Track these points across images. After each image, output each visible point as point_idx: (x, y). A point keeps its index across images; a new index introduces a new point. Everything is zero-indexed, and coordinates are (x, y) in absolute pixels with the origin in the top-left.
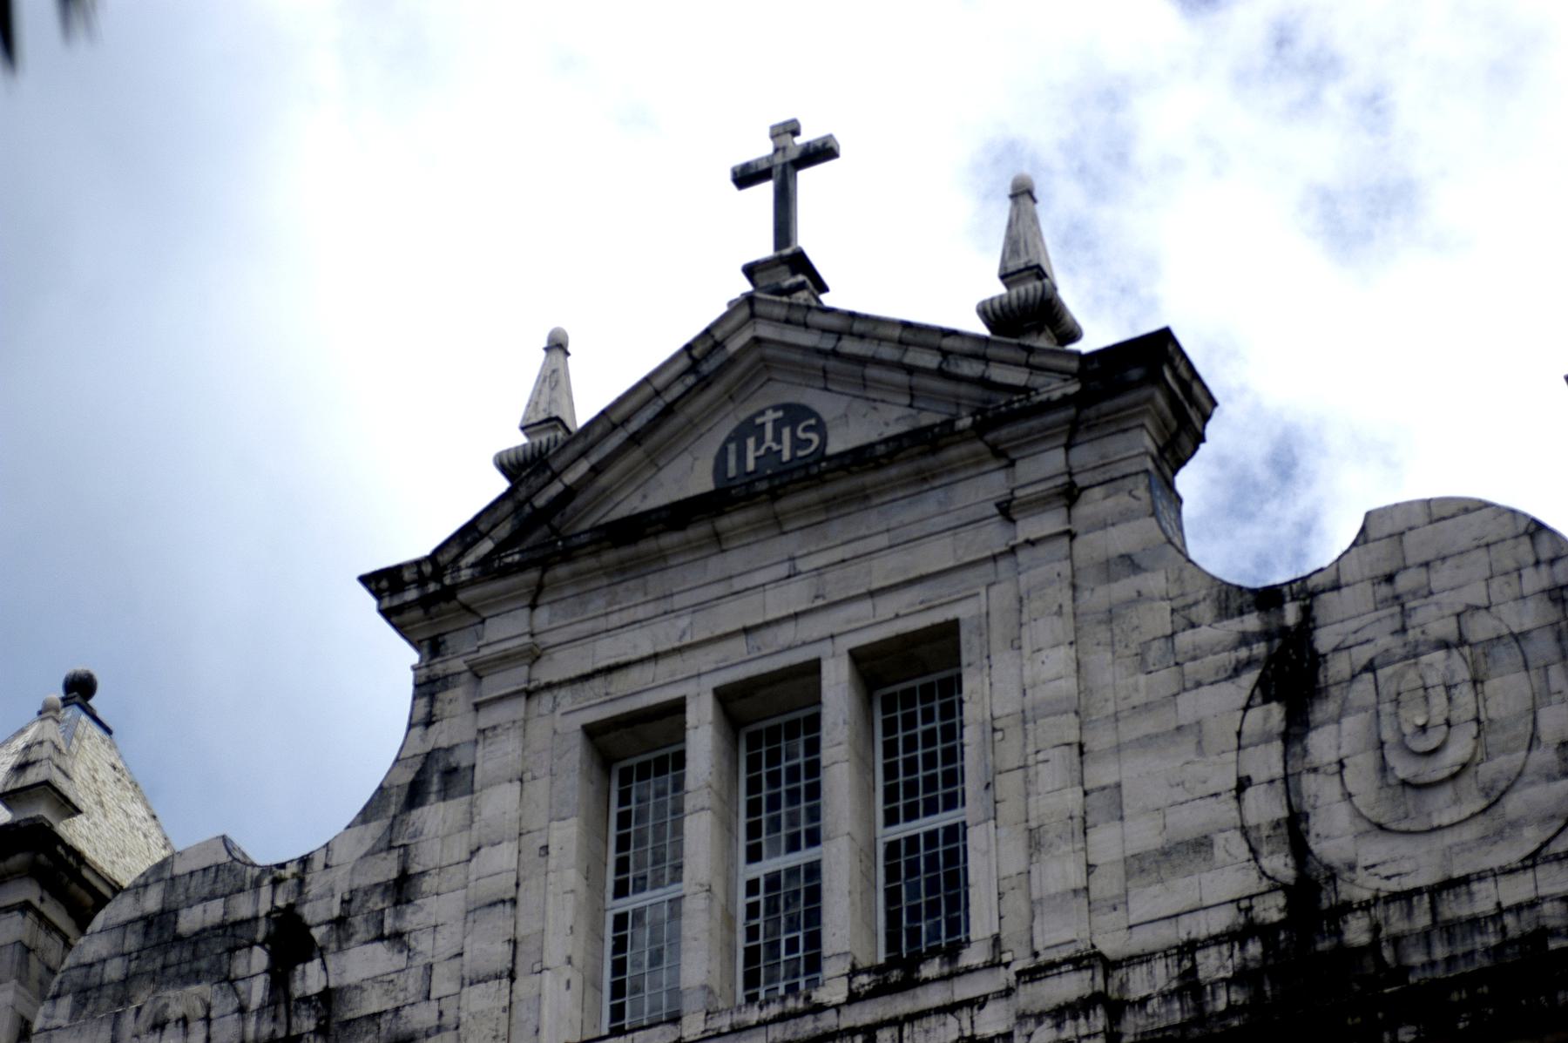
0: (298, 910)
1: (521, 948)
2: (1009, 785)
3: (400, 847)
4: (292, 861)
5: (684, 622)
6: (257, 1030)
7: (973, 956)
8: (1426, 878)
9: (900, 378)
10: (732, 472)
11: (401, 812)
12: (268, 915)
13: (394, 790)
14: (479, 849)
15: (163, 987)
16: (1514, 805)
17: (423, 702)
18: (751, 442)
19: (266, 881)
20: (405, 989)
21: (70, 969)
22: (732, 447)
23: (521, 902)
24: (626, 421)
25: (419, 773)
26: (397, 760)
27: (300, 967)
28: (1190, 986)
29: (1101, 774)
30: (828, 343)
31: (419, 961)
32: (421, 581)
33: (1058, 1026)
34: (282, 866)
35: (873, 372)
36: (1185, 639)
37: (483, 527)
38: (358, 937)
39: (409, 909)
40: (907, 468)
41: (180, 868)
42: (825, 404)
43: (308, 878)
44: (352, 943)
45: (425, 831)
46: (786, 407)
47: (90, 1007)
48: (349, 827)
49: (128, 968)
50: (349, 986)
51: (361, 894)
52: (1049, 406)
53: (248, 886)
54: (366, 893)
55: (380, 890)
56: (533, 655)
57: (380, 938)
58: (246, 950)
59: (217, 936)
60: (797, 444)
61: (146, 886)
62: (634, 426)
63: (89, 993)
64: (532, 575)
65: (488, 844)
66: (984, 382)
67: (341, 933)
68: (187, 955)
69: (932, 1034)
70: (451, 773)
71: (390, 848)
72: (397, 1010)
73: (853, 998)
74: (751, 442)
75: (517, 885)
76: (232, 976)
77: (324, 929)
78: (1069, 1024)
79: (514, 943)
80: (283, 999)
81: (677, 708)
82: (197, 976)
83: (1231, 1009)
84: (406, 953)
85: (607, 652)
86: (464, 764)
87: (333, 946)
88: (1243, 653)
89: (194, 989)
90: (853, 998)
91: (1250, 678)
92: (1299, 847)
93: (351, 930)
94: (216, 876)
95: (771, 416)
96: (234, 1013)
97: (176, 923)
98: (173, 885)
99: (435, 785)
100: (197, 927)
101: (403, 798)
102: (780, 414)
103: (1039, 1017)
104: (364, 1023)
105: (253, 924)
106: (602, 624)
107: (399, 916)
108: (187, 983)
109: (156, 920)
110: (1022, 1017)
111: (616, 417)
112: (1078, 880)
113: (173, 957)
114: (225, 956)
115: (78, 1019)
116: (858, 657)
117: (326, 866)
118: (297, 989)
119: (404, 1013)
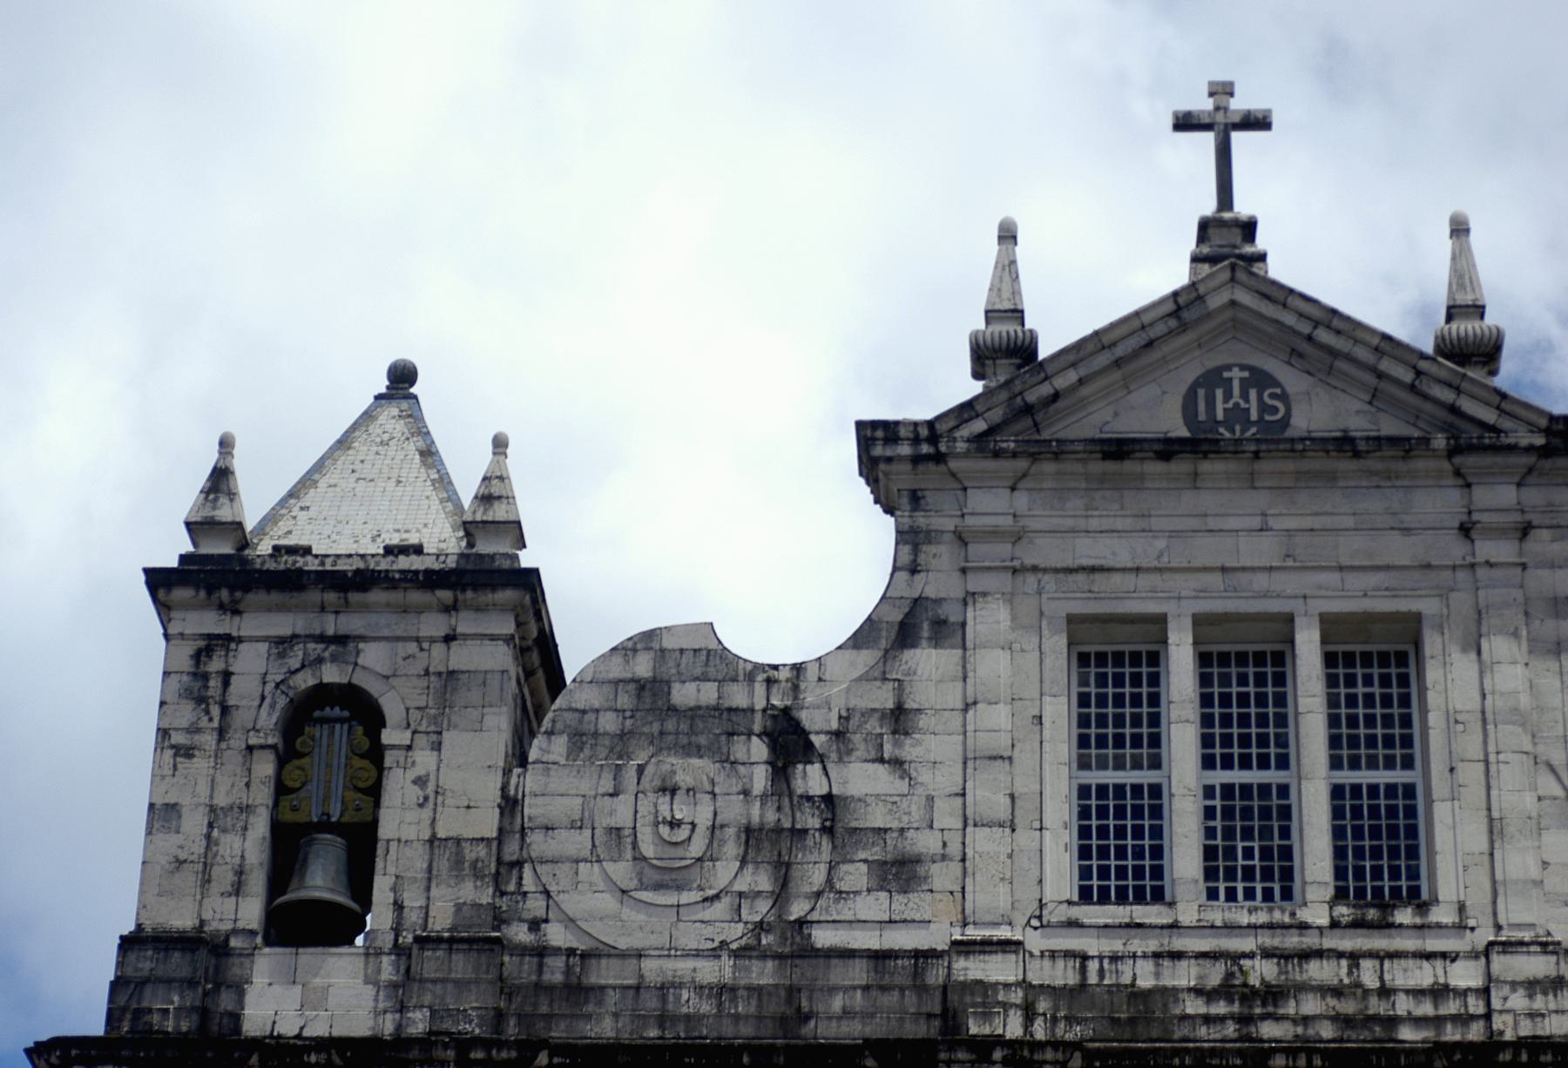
0: (795, 714)
1: (1019, 803)
2: (1471, 774)
3: (895, 680)
4: (784, 665)
5: (1161, 544)
6: (762, 816)
7: (1442, 914)
9: (1370, 379)
10: (1202, 417)
11: (892, 648)
12: (764, 711)
13: (884, 625)
14: (975, 703)
15: (665, 753)
17: (906, 549)
18: (1219, 393)
19: (761, 677)
20: (910, 813)
21: (560, 709)
22: (1201, 392)
23: (1016, 760)
24: (1114, 344)
25: (907, 615)
26: (884, 597)
27: (800, 767)
30: (1305, 328)
31: (920, 790)
32: (916, 440)
33: (1531, 996)
34: (775, 667)
35: (1341, 365)
37: (979, 408)
38: (858, 753)
39: (908, 741)
40: (1379, 466)
41: (668, 643)
43: (803, 686)
44: (853, 759)
45: (919, 672)
47: (587, 751)
48: (839, 648)
49: (623, 724)
50: (852, 797)
51: (858, 716)
52: (1512, 449)
53: (741, 677)
54: (863, 715)
55: (877, 715)
56: (1017, 537)
57: (881, 760)
58: (743, 737)
59: (714, 717)
60: (1264, 408)
61: (635, 650)
62: (1119, 351)
63: (584, 738)
64: (1022, 464)
65: (984, 701)
66: (1453, 409)
67: (841, 745)
68: (684, 727)
69: (1409, 974)
70: (940, 625)
71: (885, 679)
72: (902, 830)
73: (1335, 924)
74: (1219, 393)
75: (1013, 746)
76: (732, 758)
77: (823, 738)
78: (1539, 997)
79: (1012, 796)
80: (787, 793)
82: (699, 750)
84: (907, 780)
85: (1088, 551)
86: (952, 619)
87: (834, 756)
89: (696, 762)
93: (851, 746)
94: (708, 660)
96: (739, 793)
97: (669, 694)
98: (663, 657)
99: (926, 630)
100: (692, 704)
101: (893, 635)
102: (1246, 374)
104: (870, 835)
105: (749, 714)
106: (1081, 523)
108: (689, 755)
109: (648, 686)
111: (1106, 340)
112: (1535, 872)
113: (670, 725)
114: (723, 738)
115: (575, 760)
117: (820, 679)
118: (799, 786)
119: (910, 834)
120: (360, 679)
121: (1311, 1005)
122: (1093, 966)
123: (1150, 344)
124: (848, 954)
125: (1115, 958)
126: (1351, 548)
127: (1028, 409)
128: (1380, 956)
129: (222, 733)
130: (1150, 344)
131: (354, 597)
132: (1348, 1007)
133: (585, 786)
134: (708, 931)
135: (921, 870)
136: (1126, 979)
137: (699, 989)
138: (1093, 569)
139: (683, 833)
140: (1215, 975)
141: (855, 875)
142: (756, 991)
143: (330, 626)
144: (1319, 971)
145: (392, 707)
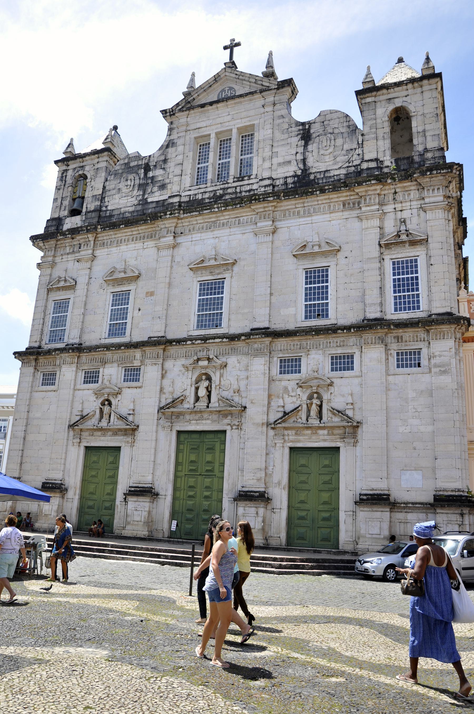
2: (260, 151)
8: (324, 169)
9: (248, 83)
16: (338, 159)
28: (286, 183)
29: (275, 150)
35: (244, 82)
36: (290, 129)
37: (180, 104)
42: (236, 87)
46: (229, 87)
57: (161, 169)
60: (231, 93)
62: (205, 89)
64: (187, 112)
70: (173, 143)
79: (182, 170)
81: (209, 135)
83: (292, 187)
85: (199, 125)
88: (299, 132)
90: (234, 182)
91: (300, 136)
92: (304, 164)
95: (227, 88)
103: (262, 187)
106: (198, 121)
107: (164, 165)
110: (260, 186)
113: (129, 170)
116: (238, 129)
118: (148, 176)
120: (85, 173)
121: (227, 197)
122: (192, 197)
123: (210, 86)
124: (152, 202)
125: (195, 195)
126: (244, 114)
127: (189, 102)
128: (241, 186)
129: (64, 185)
130: (210, 86)
131: (84, 159)
132: (233, 196)
133: (115, 182)
134: (132, 203)
135: (166, 186)
136: (197, 198)
137: (129, 212)
138: (199, 128)
139: (129, 187)
140: (212, 195)
141: (156, 189)
142: (137, 211)
143: (81, 164)
144: (229, 191)
145: (89, 176)
